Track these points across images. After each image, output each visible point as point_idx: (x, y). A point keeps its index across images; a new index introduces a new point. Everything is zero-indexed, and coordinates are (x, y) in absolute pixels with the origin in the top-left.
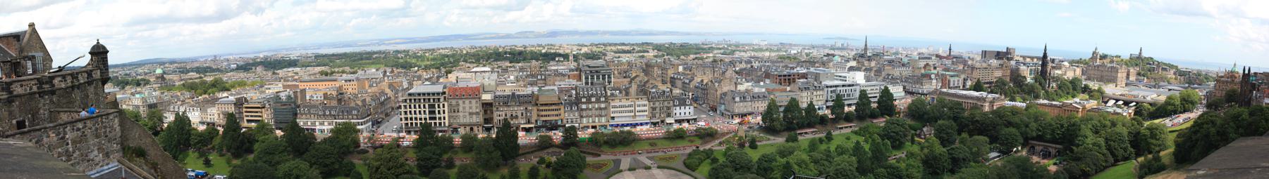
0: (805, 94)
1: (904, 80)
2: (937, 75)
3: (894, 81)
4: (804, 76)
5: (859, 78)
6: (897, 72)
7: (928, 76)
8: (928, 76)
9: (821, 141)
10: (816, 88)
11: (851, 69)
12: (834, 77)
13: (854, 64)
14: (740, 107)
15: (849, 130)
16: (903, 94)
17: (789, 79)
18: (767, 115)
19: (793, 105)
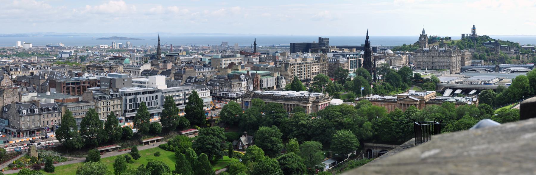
0: (101, 104)
1: (210, 83)
2: (247, 75)
3: (198, 83)
4: (95, 83)
5: (160, 82)
6: (199, 73)
7: (237, 77)
8: (237, 77)
9: (128, 159)
10: (112, 98)
11: (146, 73)
12: (131, 83)
13: (147, 67)
14: (26, 122)
15: (157, 145)
16: (210, 99)
17: (78, 88)
18: (62, 131)
19: (91, 118)
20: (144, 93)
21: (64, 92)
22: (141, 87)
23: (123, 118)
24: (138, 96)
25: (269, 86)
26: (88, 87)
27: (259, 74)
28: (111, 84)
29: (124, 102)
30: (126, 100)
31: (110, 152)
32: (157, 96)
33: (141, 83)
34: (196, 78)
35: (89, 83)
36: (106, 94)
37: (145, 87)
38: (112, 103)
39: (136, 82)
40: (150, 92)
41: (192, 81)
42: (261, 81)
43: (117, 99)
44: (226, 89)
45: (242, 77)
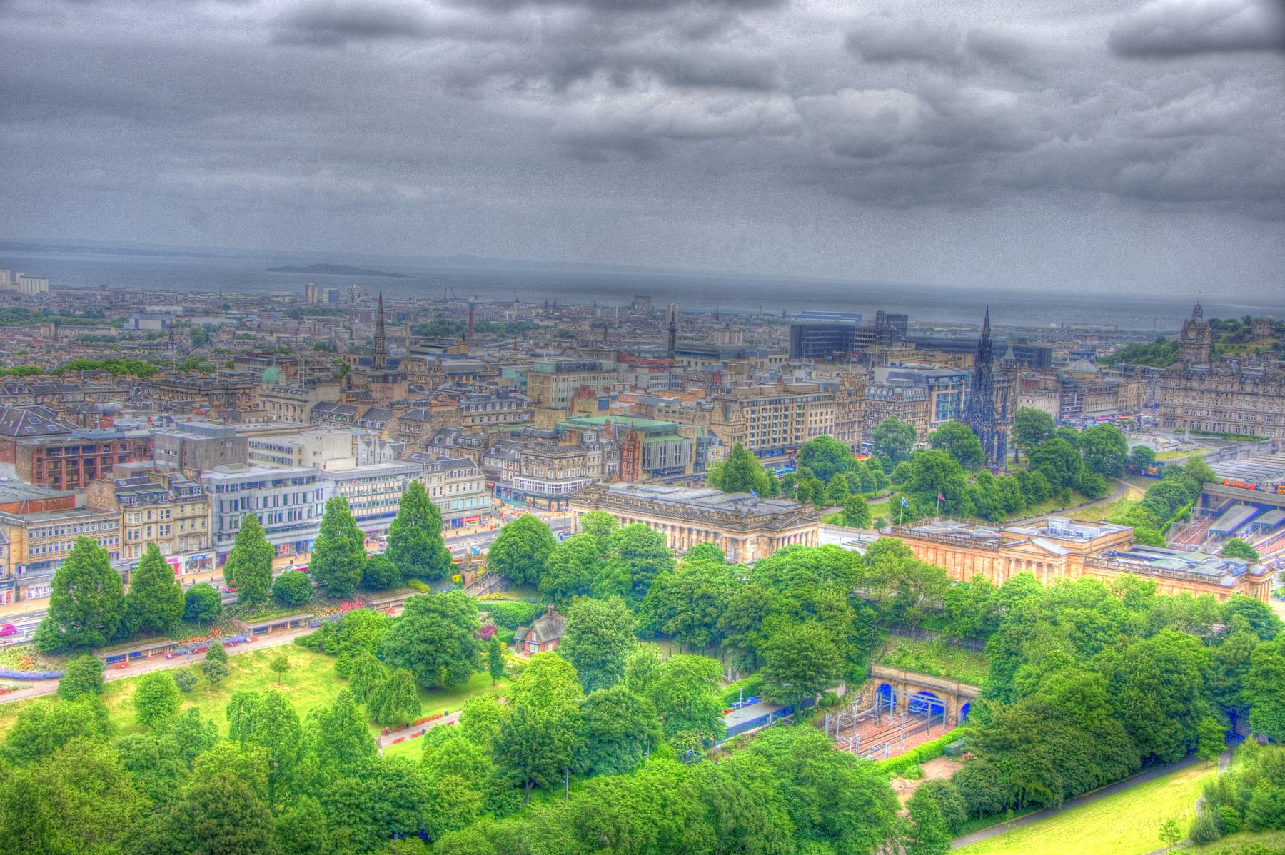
4: (144, 448)
20: (278, 482)
21: (39, 473)
22: (283, 461)
23: (212, 555)
24: (259, 493)
25: (671, 463)
26: (122, 460)
27: (641, 429)
28: (183, 453)
29: (215, 509)
30: (222, 502)
31: (145, 658)
32: (318, 494)
33: (281, 449)
34: (459, 433)
35: (124, 447)
36: (159, 486)
37: (288, 462)
38: (176, 512)
39: (270, 447)
40: (298, 481)
41: (449, 441)
42: (646, 451)
43: (194, 501)
44: (541, 471)
45: (589, 438)
